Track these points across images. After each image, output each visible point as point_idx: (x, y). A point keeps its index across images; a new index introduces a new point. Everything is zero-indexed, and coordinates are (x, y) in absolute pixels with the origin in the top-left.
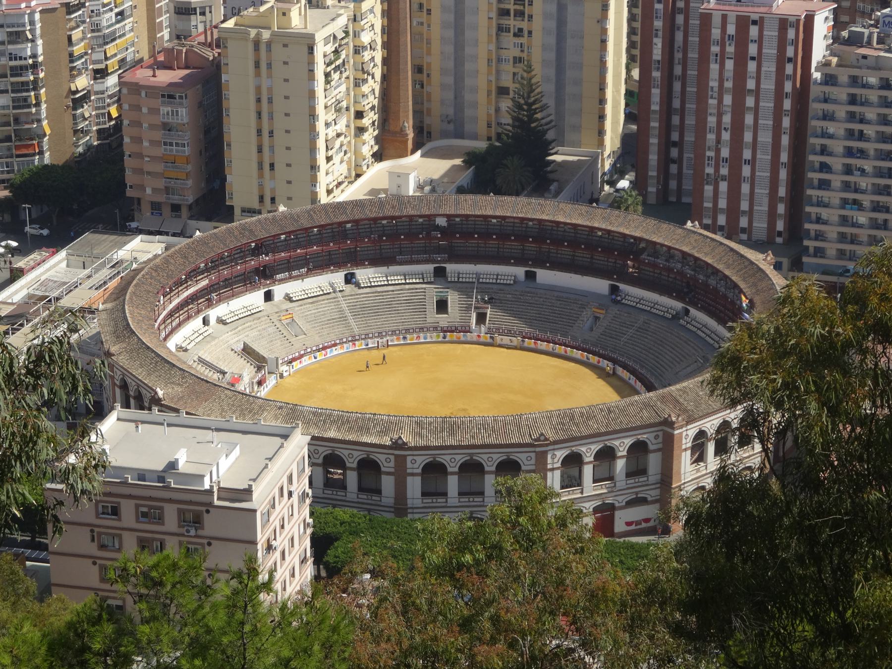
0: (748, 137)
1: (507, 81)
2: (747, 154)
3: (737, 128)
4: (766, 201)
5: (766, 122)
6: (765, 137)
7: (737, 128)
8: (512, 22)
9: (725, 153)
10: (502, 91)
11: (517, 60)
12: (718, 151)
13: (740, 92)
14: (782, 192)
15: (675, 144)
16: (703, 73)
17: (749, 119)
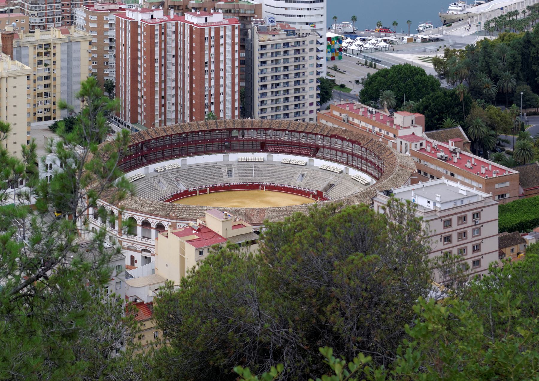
0: (222, 82)
1: (43, 90)
2: (222, 90)
3: (218, 78)
4: (230, 110)
5: (229, 73)
6: (229, 81)
7: (218, 78)
8: (44, 58)
9: (213, 92)
10: (40, 95)
11: (46, 78)
12: (210, 91)
13: (217, 62)
14: (237, 105)
15: (163, 97)
16: (202, 56)
17: (222, 74)
